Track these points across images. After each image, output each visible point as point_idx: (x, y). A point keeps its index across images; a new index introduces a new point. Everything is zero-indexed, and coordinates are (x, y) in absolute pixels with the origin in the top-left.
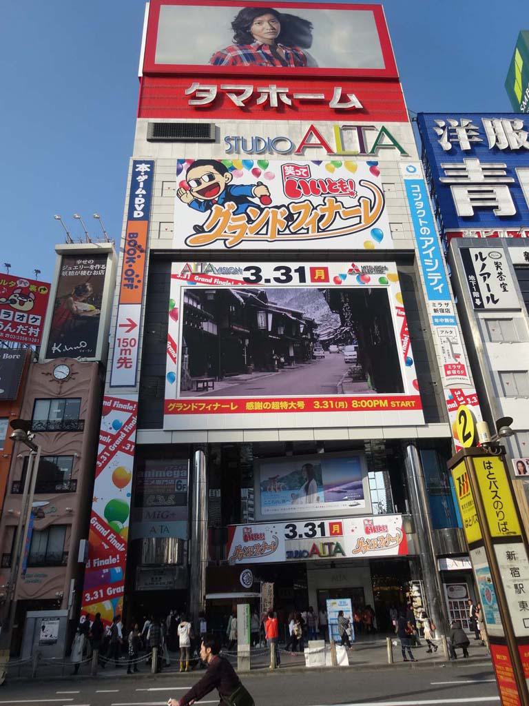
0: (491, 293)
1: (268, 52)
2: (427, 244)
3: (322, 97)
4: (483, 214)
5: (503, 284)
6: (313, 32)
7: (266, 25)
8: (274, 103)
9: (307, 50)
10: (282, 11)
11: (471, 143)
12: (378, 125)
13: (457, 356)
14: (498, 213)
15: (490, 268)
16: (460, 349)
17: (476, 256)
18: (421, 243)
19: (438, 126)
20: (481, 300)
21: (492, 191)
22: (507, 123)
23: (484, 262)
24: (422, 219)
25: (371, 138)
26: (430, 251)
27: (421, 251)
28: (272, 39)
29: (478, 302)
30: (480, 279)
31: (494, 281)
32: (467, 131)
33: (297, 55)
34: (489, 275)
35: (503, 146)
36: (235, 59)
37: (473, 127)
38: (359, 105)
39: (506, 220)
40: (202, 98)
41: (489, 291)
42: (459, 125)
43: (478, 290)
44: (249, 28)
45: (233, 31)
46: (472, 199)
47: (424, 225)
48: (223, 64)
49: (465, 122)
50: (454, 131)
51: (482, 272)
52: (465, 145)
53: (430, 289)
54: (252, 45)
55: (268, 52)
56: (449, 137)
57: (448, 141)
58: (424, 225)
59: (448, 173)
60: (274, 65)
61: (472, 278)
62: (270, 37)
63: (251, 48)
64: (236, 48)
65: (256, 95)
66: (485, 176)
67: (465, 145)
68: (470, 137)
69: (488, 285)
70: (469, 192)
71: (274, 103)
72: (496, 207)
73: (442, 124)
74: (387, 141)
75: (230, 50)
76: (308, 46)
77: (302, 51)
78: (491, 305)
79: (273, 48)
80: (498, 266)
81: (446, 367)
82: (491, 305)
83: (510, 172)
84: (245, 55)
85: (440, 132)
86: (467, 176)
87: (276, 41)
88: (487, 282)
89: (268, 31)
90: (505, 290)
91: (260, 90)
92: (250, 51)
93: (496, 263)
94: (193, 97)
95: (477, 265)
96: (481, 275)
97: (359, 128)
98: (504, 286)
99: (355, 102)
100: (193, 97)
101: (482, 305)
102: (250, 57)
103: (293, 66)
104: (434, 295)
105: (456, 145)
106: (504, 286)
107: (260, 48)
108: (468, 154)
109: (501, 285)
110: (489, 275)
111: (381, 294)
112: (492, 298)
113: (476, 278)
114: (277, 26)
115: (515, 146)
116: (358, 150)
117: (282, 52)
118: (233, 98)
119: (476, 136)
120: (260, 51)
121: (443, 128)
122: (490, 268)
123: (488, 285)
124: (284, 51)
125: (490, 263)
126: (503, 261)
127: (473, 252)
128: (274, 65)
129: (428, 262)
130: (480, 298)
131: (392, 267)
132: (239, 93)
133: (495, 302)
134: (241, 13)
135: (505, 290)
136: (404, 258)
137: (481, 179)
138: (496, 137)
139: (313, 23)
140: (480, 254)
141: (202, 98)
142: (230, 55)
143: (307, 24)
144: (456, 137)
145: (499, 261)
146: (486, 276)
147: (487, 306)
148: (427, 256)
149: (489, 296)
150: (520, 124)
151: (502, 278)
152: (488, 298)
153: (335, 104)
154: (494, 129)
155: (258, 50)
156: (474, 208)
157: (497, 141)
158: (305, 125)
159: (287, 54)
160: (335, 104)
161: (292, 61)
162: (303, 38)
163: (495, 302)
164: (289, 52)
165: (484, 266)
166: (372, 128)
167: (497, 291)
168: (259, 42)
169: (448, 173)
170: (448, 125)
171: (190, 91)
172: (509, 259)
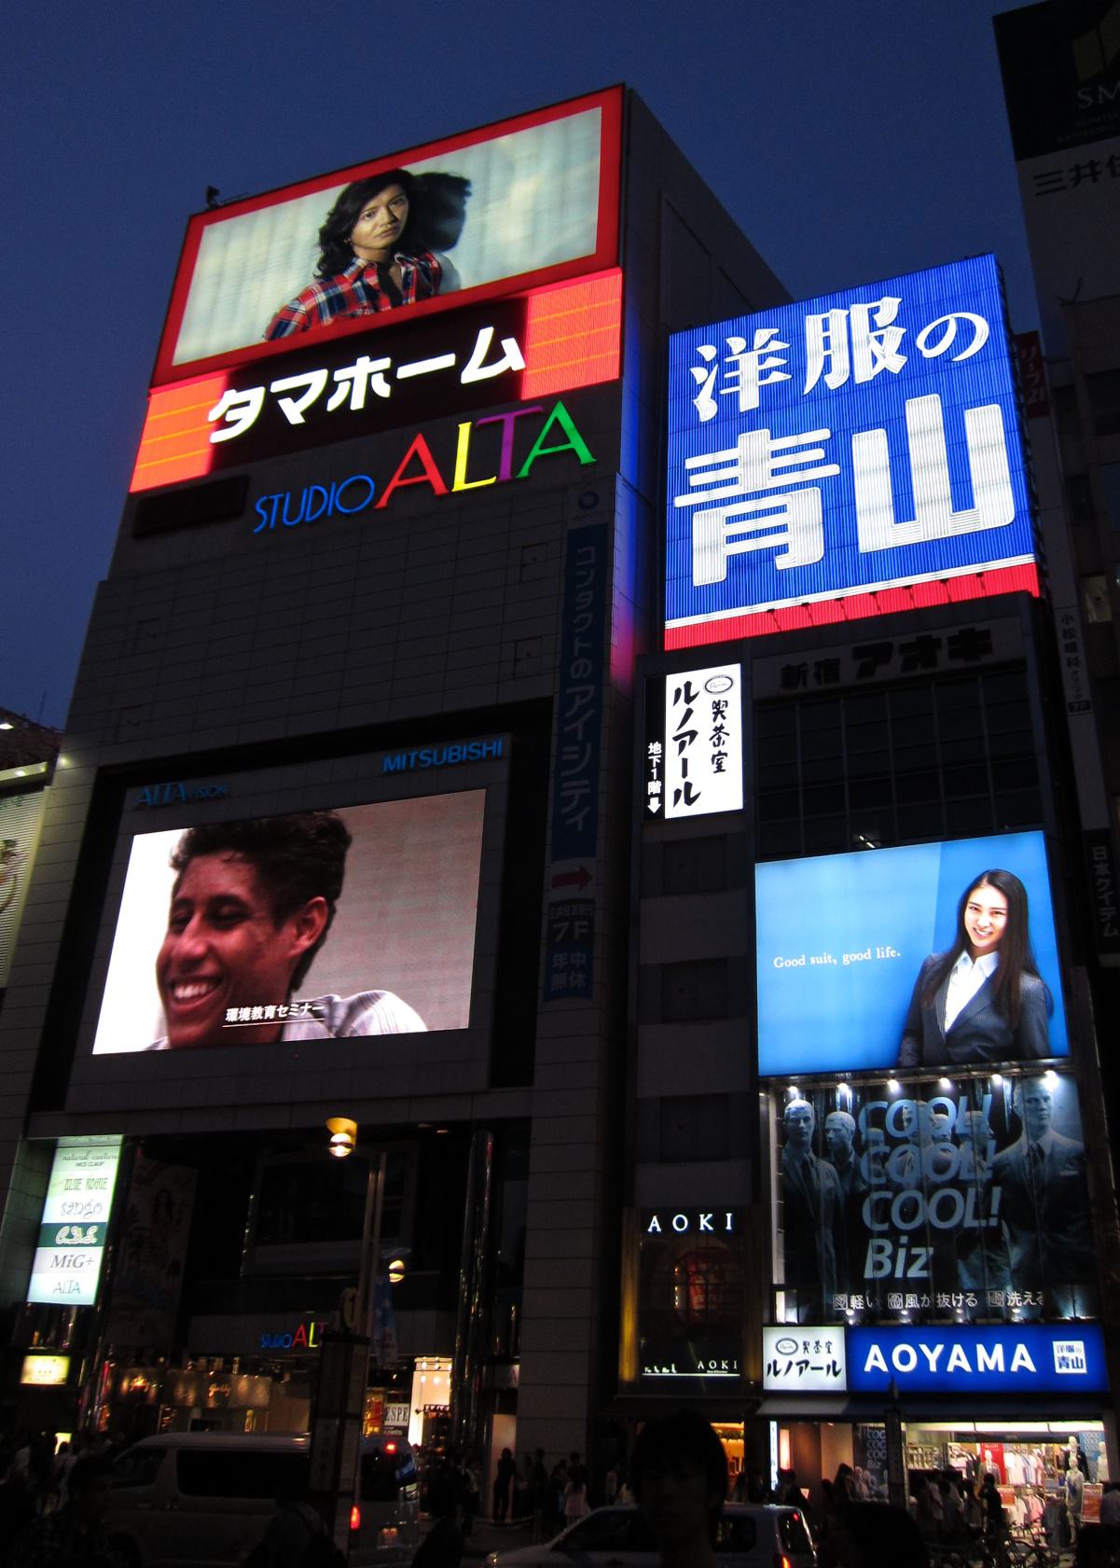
0: (687, 779)
1: (373, 280)
5: (720, 753)
6: (471, 206)
7: (382, 216)
8: (358, 403)
9: (448, 254)
10: (417, 168)
11: (764, 391)
14: (782, 562)
15: (702, 720)
17: (678, 692)
19: (701, 362)
20: (662, 800)
22: (859, 311)
23: (692, 705)
28: (383, 248)
30: (672, 746)
31: (700, 752)
32: (762, 359)
33: (425, 270)
34: (693, 734)
35: (835, 380)
36: (315, 313)
37: (776, 346)
39: (805, 578)
41: (685, 774)
43: (661, 777)
44: (349, 232)
45: (319, 249)
48: (286, 334)
50: (735, 366)
51: (686, 729)
52: (749, 399)
54: (346, 275)
55: (373, 280)
57: (716, 395)
60: (377, 309)
62: (381, 243)
63: (345, 280)
64: (316, 287)
65: (331, 387)
66: (775, 472)
67: (749, 399)
69: (685, 762)
70: (731, 520)
72: (783, 549)
75: (306, 295)
76: (449, 242)
80: (718, 710)
83: (838, 451)
84: (330, 301)
85: (699, 373)
87: (391, 249)
88: (684, 755)
89: (384, 229)
90: (720, 769)
93: (716, 705)
94: (223, 424)
96: (676, 739)
98: (718, 762)
100: (223, 424)
101: (662, 810)
103: (411, 300)
105: (727, 404)
107: (360, 275)
108: (751, 421)
109: (714, 756)
110: (693, 734)
113: (663, 748)
114: (400, 212)
115: (864, 374)
118: (286, 405)
119: (777, 369)
120: (359, 284)
121: (708, 366)
122: (702, 720)
123: (685, 762)
124: (403, 269)
125: (702, 706)
128: (377, 309)
130: (661, 796)
132: (297, 394)
133: (689, 801)
134: (342, 200)
135: (720, 769)
138: (828, 360)
140: (688, 685)
143: (459, 186)
144: (735, 382)
145: (722, 697)
146: (687, 739)
149: (682, 788)
150: (889, 307)
151: (719, 739)
152: (677, 793)
155: (355, 281)
156: (736, 563)
157: (827, 367)
159: (408, 273)
161: (412, 290)
163: (689, 801)
164: (412, 268)
165: (689, 712)
167: (701, 775)
168: (360, 262)
169: (695, 480)
170: (724, 351)
171: (214, 415)
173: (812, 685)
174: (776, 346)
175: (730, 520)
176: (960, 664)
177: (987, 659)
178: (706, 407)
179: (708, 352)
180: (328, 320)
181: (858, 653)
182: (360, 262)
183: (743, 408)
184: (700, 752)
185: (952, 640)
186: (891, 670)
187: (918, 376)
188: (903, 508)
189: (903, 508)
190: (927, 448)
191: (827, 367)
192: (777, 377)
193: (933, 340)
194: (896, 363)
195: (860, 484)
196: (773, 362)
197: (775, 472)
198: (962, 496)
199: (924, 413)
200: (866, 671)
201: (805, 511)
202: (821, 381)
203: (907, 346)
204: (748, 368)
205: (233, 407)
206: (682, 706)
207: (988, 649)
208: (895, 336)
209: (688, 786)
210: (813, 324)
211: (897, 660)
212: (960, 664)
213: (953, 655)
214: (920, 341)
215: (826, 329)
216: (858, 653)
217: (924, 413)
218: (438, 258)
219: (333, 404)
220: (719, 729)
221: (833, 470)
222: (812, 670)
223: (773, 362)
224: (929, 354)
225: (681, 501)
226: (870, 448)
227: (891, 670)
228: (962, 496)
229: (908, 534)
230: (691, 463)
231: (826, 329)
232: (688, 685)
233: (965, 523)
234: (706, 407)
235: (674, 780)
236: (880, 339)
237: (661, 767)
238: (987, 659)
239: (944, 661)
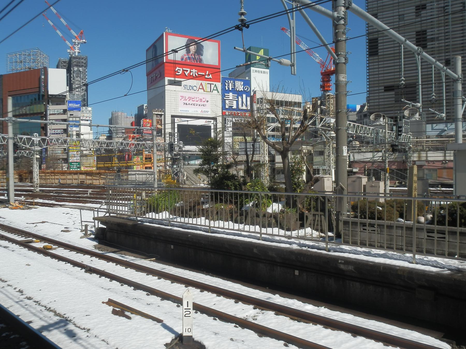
3: (204, 74)
8: (194, 75)
12: (214, 83)
14: (233, 108)
19: (226, 82)
22: (240, 82)
25: (213, 86)
33: (199, 58)
36: (186, 58)
37: (233, 83)
38: (211, 78)
40: (179, 72)
52: (230, 89)
56: (228, 86)
59: (226, 96)
62: (194, 51)
65: (191, 72)
67: (230, 89)
68: (232, 86)
71: (194, 75)
74: (215, 88)
75: (185, 55)
76: (202, 56)
77: (201, 57)
78: (228, 130)
79: (194, 55)
82: (228, 130)
87: (195, 52)
91: (191, 71)
92: (190, 56)
97: (211, 84)
99: (210, 76)
102: (189, 58)
105: (229, 88)
108: (230, 91)
116: (210, 91)
117: (197, 57)
118: (185, 72)
136: (215, 119)
139: (204, 47)
141: (179, 72)
142: (185, 57)
144: (229, 86)
150: (242, 83)
158: (200, 82)
162: (202, 52)
166: (213, 84)
168: (191, 53)
169: (226, 96)
170: (228, 82)
171: (176, 70)
174: (233, 83)
178: (227, 89)
179: (227, 82)
180: (188, 61)
182: (191, 53)
187: (244, 92)
188: (242, 106)
189: (242, 106)
190: (244, 100)
192: (233, 87)
199: (244, 96)
201: (235, 103)
203: (243, 88)
204: (230, 85)
205: (178, 70)
208: (242, 86)
210: (236, 82)
217: (244, 96)
218: (201, 57)
219: (191, 74)
221: (237, 99)
234: (227, 89)
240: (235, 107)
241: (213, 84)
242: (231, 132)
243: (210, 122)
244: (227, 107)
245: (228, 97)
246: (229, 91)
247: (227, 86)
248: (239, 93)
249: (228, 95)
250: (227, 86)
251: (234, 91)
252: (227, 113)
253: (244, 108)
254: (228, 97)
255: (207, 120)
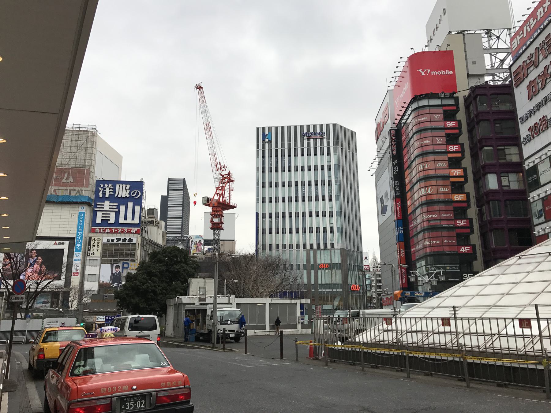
2: (79, 234)
4: (105, 222)
13: (77, 270)
14: (109, 222)
15: (96, 244)
16: (79, 268)
18: (78, 234)
19: (100, 187)
21: (110, 214)
22: (124, 186)
24: (81, 226)
26: (80, 237)
27: (77, 236)
29: (89, 254)
30: (92, 247)
31: (95, 248)
32: (110, 189)
34: (95, 246)
35: (119, 196)
37: (112, 188)
39: (111, 225)
42: (108, 187)
46: (102, 217)
47: (80, 228)
49: (110, 185)
50: (106, 189)
52: (107, 196)
53: (76, 249)
56: (103, 191)
58: (80, 228)
59: (98, 206)
61: (89, 247)
66: (110, 208)
67: (107, 196)
68: (110, 192)
70: (102, 214)
72: (109, 220)
73: (102, 186)
80: (98, 243)
81: (74, 273)
82: (92, 255)
83: (118, 207)
85: (100, 189)
86: (103, 208)
90: (98, 251)
93: (98, 242)
95: (92, 242)
98: (98, 250)
101: (89, 255)
104: (77, 251)
106: (98, 250)
108: (107, 199)
110: (95, 246)
111: (63, 251)
112: (93, 254)
115: (123, 196)
121: (102, 188)
122: (96, 244)
125: (96, 242)
126: (100, 242)
127: (93, 238)
129: (78, 240)
131: (67, 243)
133: (93, 255)
135: (98, 251)
136: (71, 240)
137: (108, 209)
140: (94, 239)
144: (105, 192)
147: (91, 256)
148: (78, 239)
150: (128, 187)
153: (64, 180)
154: (119, 190)
157: (118, 194)
160: (64, 180)
163: (93, 255)
165: (94, 243)
166: (75, 190)
167: (95, 251)
169: (98, 206)
170: (104, 186)
172: (102, 240)
173: (111, 242)
174: (112, 188)
175: (102, 214)
176: (129, 242)
177: (132, 242)
178: (101, 195)
179: (102, 186)
181: (117, 239)
183: (106, 197)
184: (95, 248)
185: (128, 239)
186: (120, 242)
187: (130, 199)
188: (126, 218)
189: (126, 218)
191: (118, 194)
192: (111, 193)
193: (133, 194)
194: (128, 196)
195: (120, 213)
196: (111, 190)
197: (110, 208)
198: (133, 218)
199: (130, 205)
200: (117, 241)
201: (113, 215)
202: (117, 195)
203: (129, 194)
204: (108, 190)
206: (93, 242)
207: (132, 241)
208: (128, 191)
209: (93, 253)
210: (118, 186)
211: (121, 240)
212: (129, 242)
213: (128, 241)
214: (132, 194)
215: (119, 187)
216: (117, 239)
217: (130, 205)
220: (98, 246)
221: (117, 210)
222: (111, 240)
223: (111, 190)
224: (132, 196)
225: (96, 209)
226: (122, 208)
227: (120, 242)
228: (133, 218)
229: (125, 222)
230: (98, 204)
231: (119, 187)
232: (94, 239)
233: (133, 222)
234: (101, 195)
235: (91, 252)
236: (126, 191)
237: (90, 249)
238: (132, 242)
239: (127, 242)
240: (112, 221)
241: (75, 190)
242: (99, 258)
243: (63, 244)
244: (99, 221)
245: (102, 207)
246: (104, 199)
247: (101, 192)
248: (123, 201)
249: (103, 204)
250: (101, 192)
251: (112, 198)
252: (97, 230)
253: (129, 221)
254: (102, 207)
255: (57, 242)
